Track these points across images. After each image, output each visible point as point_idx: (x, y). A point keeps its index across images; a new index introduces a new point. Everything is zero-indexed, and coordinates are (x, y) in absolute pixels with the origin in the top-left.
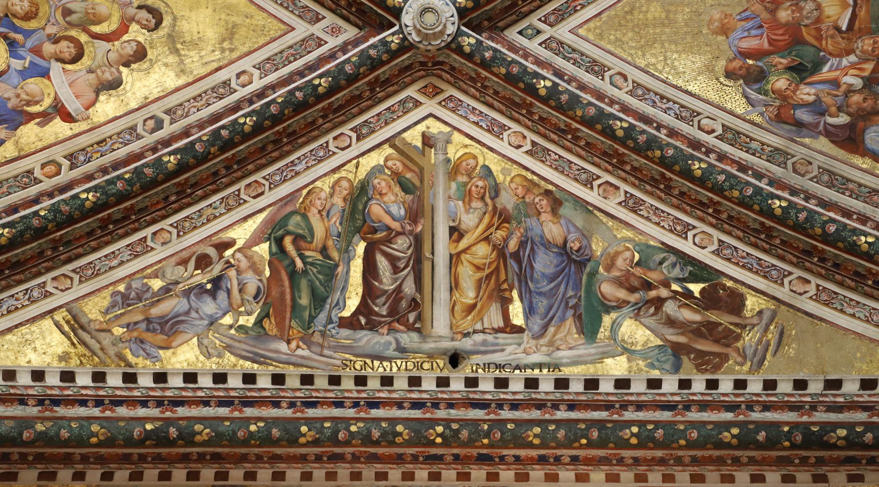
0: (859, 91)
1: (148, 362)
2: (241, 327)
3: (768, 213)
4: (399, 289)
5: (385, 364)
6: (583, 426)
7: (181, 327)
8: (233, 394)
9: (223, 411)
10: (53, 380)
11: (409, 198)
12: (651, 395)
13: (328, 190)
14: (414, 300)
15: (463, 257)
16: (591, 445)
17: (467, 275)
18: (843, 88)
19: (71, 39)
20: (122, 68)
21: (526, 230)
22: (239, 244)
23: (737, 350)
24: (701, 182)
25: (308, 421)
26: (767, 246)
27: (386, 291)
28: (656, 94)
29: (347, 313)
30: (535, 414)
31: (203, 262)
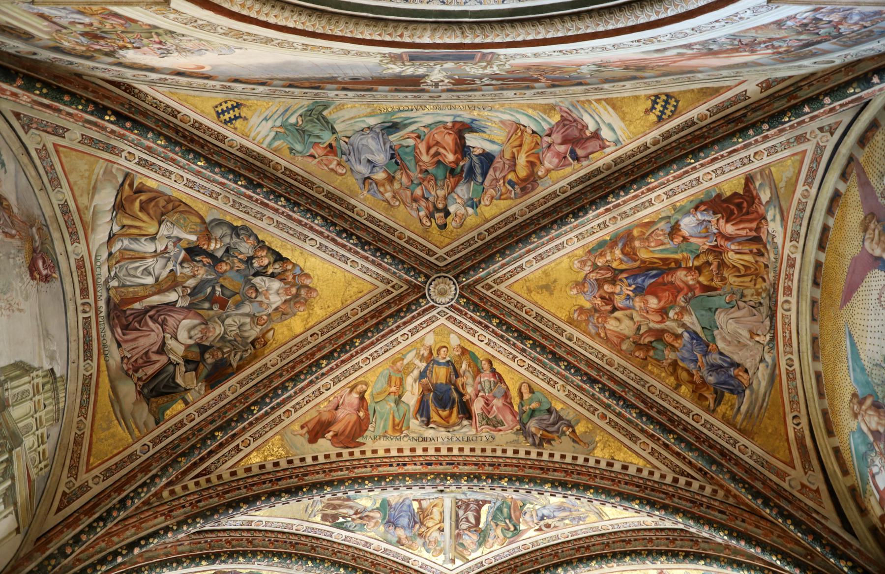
4: (465, 512)
11: (461, 541)
31: (548, 526)
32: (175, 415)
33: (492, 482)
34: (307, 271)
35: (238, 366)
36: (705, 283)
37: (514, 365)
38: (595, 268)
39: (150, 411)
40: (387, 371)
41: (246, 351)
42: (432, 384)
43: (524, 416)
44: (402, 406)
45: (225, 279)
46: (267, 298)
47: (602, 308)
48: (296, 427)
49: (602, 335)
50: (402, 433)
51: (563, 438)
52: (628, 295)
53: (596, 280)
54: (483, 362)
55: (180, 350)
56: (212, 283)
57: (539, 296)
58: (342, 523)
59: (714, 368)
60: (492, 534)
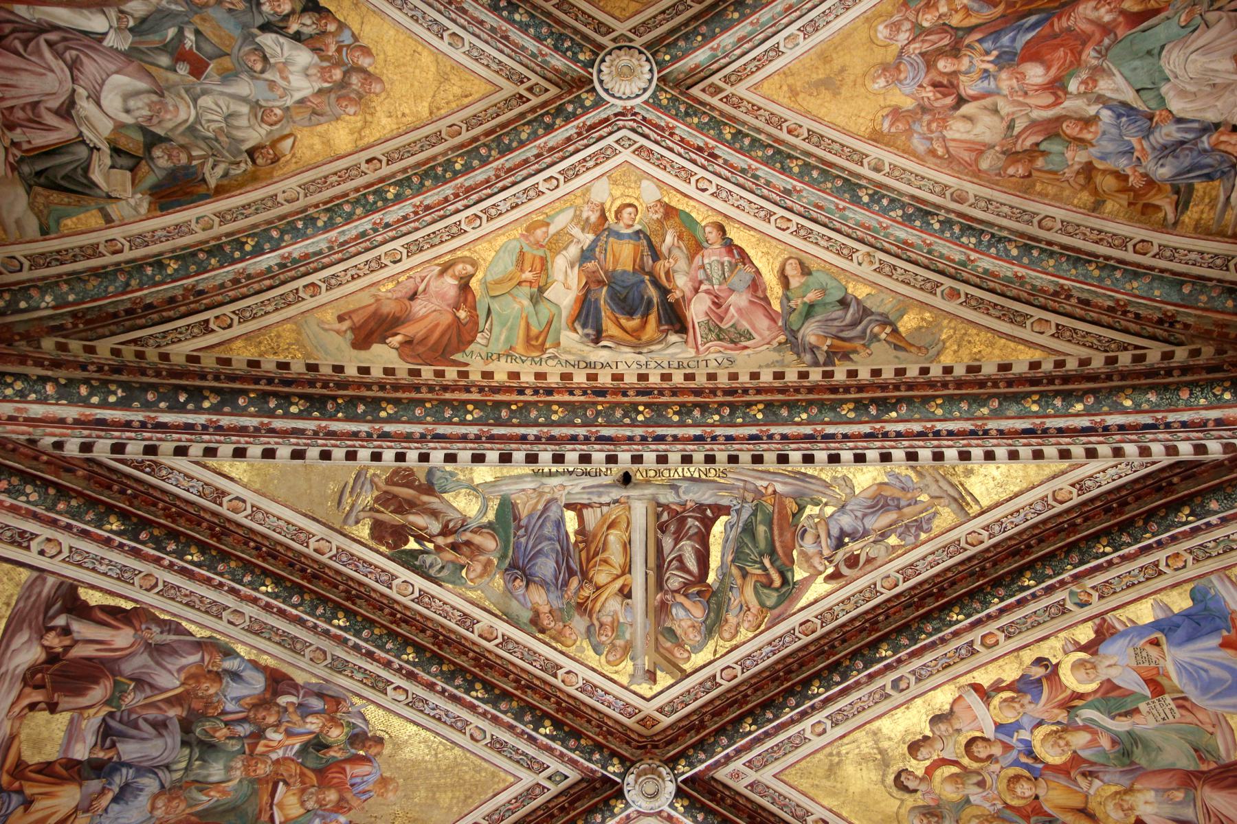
0: (269, 726)
1: (897, 471)
2: (817, 504)
3: (350, 613)
4: (677, 541)
5: (688, 475)
6: (514, 421)
7: (870, 503)
8: (823, 445)
9: (830, 430)
10: (977, 452)
11: (668, 624)
12: (454, 448)
13: (742, 629)
14: (663, 532)
15: (619, 572)
16: (508, 404)
17: (615, 555)
18: (282, 729)
19: (977, 759)
20: (930, 734)
21: (562, 596)
22: (821, 578)
23: (378, 488)
24: (407, 642)
25: (756, 423)
26: (350, 583)
27: (689, 539)
28: (445, 723)
29: (723, 519)
30: (556, 431)
31: (853, 561)
32: (83, 233)
33: (732, 413)
34: (364, 42)
35: (217, 187)
36: (1136, 9)
37: (770, 229)
38: (919, 32)
39: (31, 205)
40: (515, 245)
41: (238, 163)
42: (606, 273)
43: (793, 317)
44: (545, 311)
45: (204, 20)
46: (285, 79)
47: (936, 104)
48: (330, 316)
49: (940, 152)
50: (544, 352)
51: (875, 346)
52: (986, 71)
53: (922, 54)
54: (708, 229)
55: (106, 127)
56: (180, 19)
57: (813, 99)
58: (414, 554)
59: (1169, 150)
60: (735, 599)
